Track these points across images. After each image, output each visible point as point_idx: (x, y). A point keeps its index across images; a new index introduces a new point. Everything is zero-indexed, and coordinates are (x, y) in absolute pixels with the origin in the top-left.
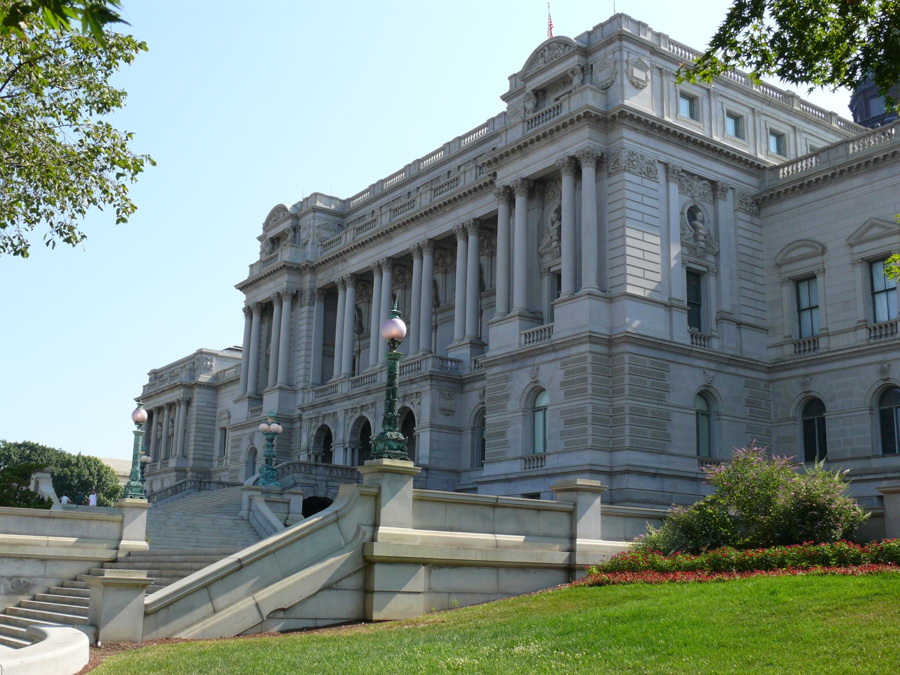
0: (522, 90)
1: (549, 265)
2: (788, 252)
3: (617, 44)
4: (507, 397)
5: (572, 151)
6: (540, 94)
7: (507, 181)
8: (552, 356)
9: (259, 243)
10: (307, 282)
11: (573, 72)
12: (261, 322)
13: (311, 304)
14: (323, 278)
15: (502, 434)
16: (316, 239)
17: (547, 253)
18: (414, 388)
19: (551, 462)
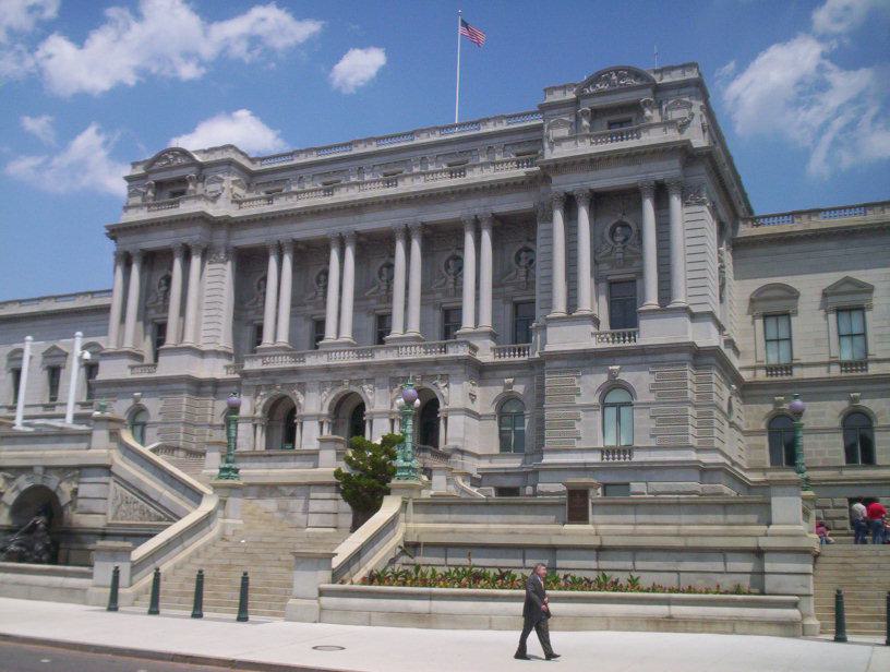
0: (576, 102)
1: (607, 273)
2: (762, 292)
3: (693, 89)
4: (577, 392)
5: (659, 176)
6: (596, 114)
7: (569, 188)
8: (639, 359)
9: (127, 184)
10: (220, 238)
11: (644, 102)
12: (141, 273)
13: (224, 262)
14: (249, 238)
15: (571, 426)
16: (230, 195)
17: (605, 262)
18: (438, 370)
19: (638, 457)
